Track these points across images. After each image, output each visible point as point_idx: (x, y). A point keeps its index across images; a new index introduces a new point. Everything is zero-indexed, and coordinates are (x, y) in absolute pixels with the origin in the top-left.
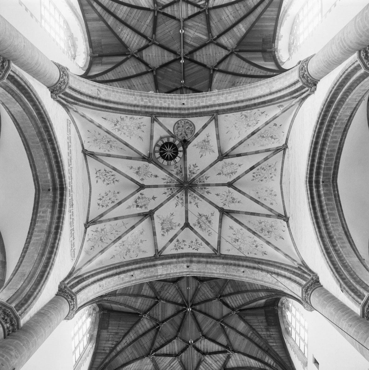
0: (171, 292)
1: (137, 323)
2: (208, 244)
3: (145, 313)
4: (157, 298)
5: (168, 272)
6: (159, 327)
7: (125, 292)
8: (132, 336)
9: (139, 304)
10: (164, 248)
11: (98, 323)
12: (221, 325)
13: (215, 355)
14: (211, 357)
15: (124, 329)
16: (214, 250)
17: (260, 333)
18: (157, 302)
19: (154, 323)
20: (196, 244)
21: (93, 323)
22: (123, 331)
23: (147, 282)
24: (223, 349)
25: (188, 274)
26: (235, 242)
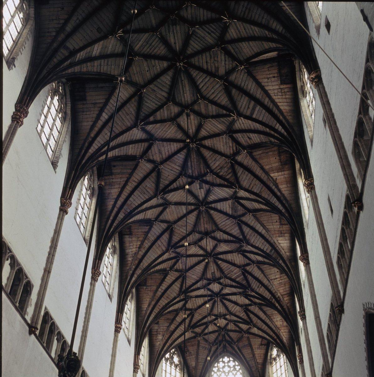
14: (203, 28)
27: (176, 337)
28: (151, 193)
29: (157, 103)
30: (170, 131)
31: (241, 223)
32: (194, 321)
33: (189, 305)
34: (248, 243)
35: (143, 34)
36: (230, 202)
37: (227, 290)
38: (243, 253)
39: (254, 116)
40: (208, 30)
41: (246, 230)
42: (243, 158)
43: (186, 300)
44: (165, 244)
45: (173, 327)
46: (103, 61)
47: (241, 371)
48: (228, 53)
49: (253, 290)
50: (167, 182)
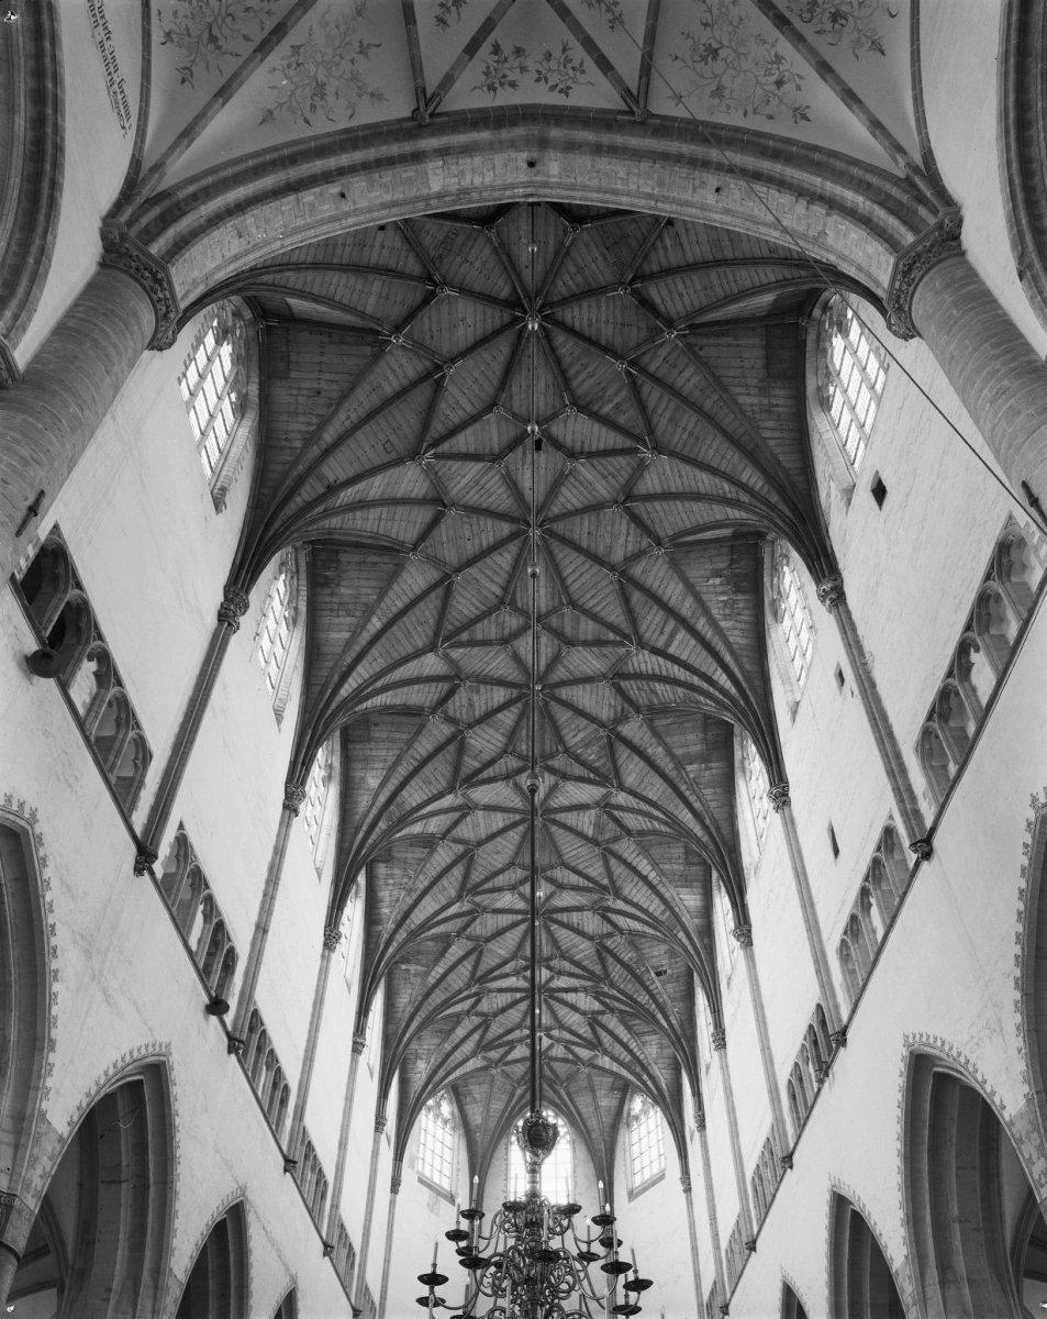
0: (476, 263)
1: (376, 358)
2: (605, 65)
3: (397, 329)
4: (429, 278)
5: (466, 182)
6: (444, 376)
7: (322, 259)
8: (363, 400)
9: (375, 299)
10: (447, 81)
11: (255, 358)
12: (629, 374)
13: (603, 461)
14: (593, 466)
15: (338, 377)
16: (626, 93)
17: (741, 399)
18: (433, 294)
19: (427, 363)
20: (561, 68)
21: (237, 359)
22: (334, 386)
23: (395, 222)
24: (628, 443)
25: (532, 195)
26: (704, 59)
27: (452, 1065)
28: (444, 783)
29: (479, 605)
30: (497, 663)
31: (608, 854)
32: (489, 1036)
33: (484, 1006)
34: (618, 894)
35: (473, 463)
36: (593, 812)
37: (562, 982)
38: (604, 913)
39: (671, 650)
40: (602, 470)
41: (619, 870)
42: (633, 729)
43: (478, 997)
44: (457, 885)
45: (448, 1047)
46: (386, 509)
47: (568, 1137)
48: (636, 520)
49: (612, 985)
50: (476, 764)
